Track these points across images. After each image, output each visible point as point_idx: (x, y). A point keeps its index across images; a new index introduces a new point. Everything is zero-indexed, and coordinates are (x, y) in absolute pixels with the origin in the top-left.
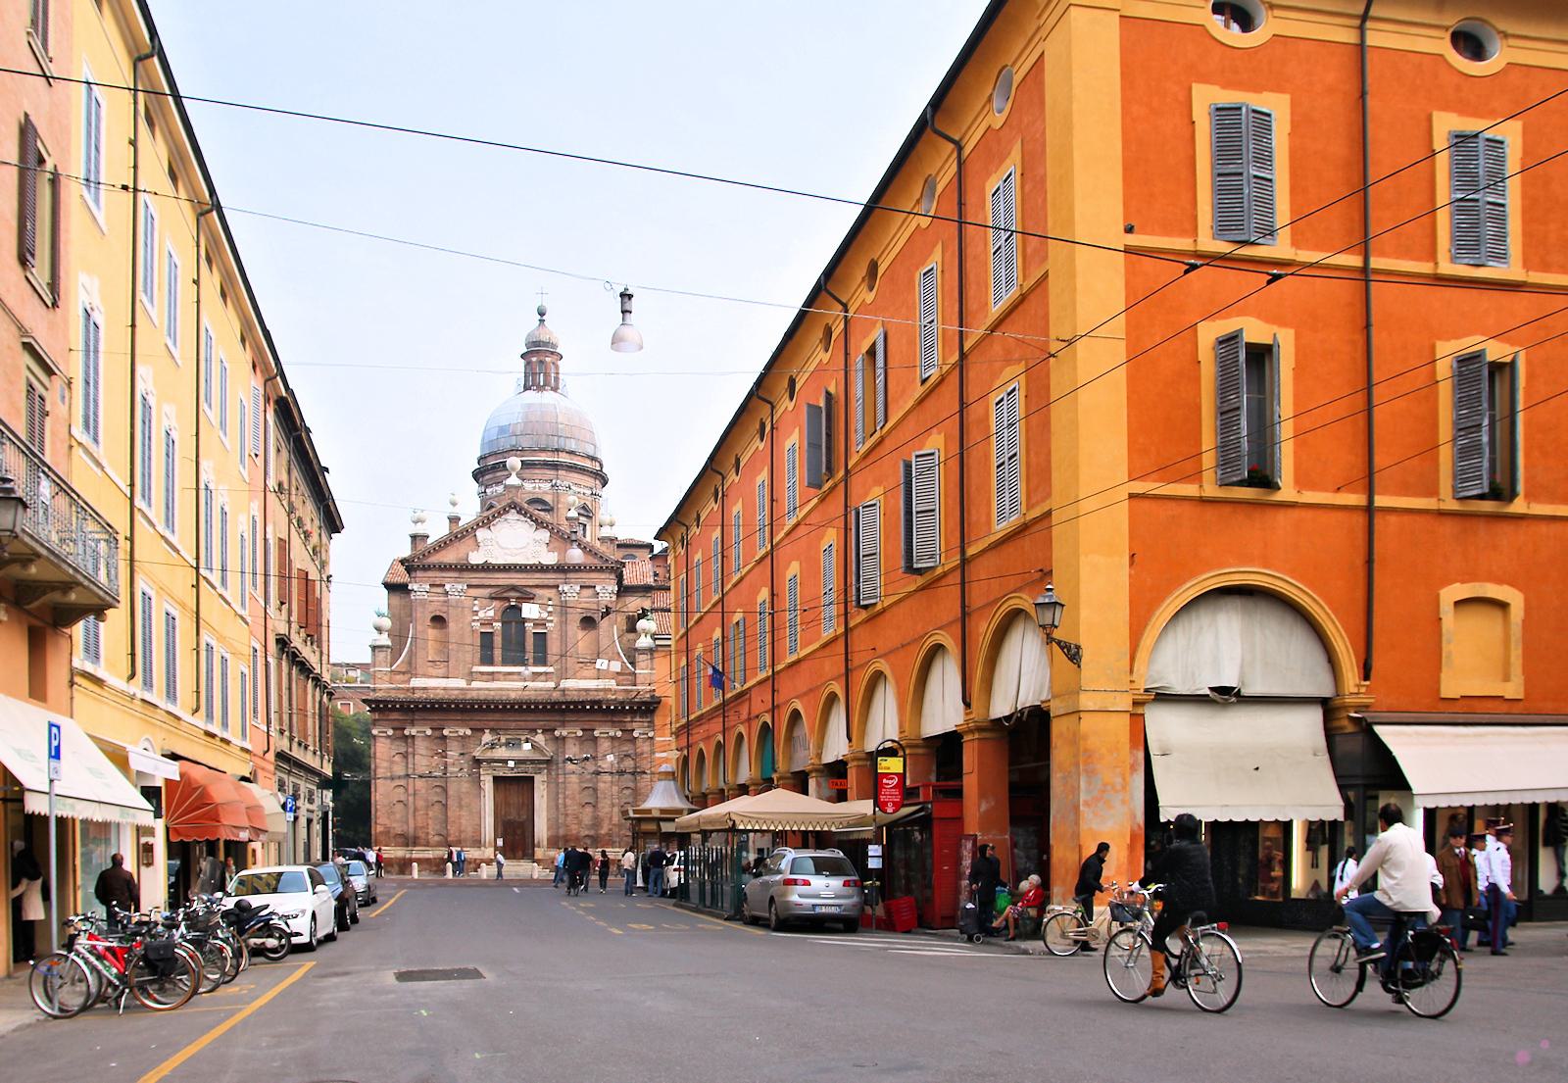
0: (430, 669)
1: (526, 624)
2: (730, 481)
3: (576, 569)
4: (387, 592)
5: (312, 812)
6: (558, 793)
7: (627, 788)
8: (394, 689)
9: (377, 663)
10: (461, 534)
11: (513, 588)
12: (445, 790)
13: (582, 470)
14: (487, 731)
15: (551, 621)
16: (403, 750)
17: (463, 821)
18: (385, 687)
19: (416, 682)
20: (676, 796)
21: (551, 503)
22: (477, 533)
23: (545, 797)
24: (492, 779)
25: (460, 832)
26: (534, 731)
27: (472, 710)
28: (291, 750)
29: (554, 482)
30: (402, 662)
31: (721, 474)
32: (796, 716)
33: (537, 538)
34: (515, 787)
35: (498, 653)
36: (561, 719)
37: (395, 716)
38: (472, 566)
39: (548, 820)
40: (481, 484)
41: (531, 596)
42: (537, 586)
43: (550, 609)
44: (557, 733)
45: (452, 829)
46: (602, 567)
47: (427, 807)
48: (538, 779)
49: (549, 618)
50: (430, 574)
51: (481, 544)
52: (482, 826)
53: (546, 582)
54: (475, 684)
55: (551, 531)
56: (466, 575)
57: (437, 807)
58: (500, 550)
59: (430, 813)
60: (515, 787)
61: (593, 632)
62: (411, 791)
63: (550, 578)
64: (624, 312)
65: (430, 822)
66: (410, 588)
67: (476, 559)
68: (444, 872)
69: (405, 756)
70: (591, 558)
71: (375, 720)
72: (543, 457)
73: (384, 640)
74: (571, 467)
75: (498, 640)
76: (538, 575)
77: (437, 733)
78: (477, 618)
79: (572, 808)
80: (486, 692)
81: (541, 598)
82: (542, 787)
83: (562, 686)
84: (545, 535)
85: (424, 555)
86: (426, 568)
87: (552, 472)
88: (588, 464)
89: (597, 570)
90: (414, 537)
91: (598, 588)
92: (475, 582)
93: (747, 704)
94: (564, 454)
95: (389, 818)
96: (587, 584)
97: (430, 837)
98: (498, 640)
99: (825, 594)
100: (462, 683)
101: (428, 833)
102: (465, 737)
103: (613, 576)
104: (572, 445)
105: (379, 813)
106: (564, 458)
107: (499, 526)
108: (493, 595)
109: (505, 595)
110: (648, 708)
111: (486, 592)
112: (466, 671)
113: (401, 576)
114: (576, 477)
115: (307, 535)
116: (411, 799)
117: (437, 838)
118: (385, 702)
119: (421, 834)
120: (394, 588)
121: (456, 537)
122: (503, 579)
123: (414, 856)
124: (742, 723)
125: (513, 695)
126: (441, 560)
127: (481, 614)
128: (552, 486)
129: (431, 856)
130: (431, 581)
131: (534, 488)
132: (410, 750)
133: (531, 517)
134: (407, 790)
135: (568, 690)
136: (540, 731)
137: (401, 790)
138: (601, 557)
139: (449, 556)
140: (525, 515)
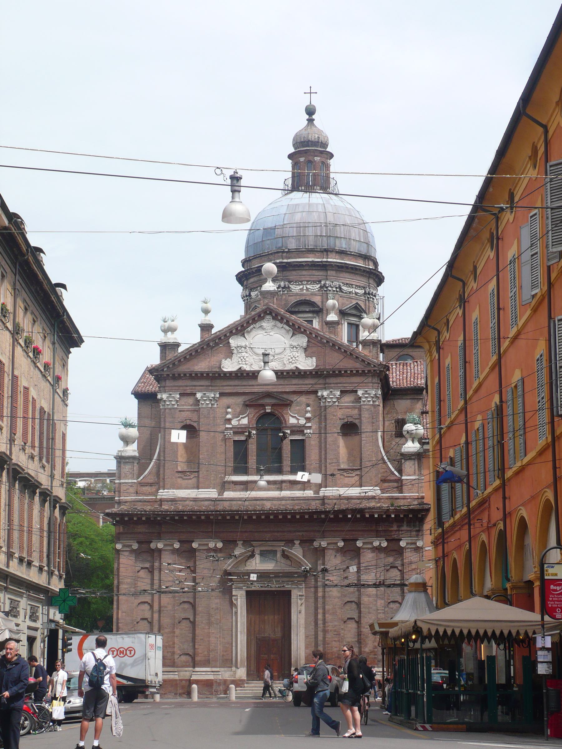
0: (179, 480)
2: (470, 288)
4: (136, 401)
5: (36, 629)
8: (140, 501)
9: (123, 475)
10: (215, 342)
12: (194, 606)
13: (354, 270)
14: (240, 543)
15: (310, 428)
16: (147, 565)
17: (212, 639)
18: (130, 499)
19: (164, 494)
20: (427, 609)
21: (319, 304)
22: (231, 341)
23: (303, 612)
25: (209, 651)
26: (290, 542)
28: (8, 566)
29: (323, 282)
30: (150, 473)
31: (461, 280)
32: (523, 525)
33: (295, 344)
34: (270, 603)
37: (141, 529)
38: (225, 373)
39: (307, 637)
40: (245, 287)
42: (294, 393)
43: (308, 415)
44: (316, 544)
45: (200, 648)
47: (173, 626)
50: (180, 383)
51: (235, 351)
52: (234, 644)
53: (304, 388)
54: (228, 494)
55: (309, 336)
56: (218, 382)
57: (185, 625)
58: (255, 357)
59: (177, 632)
60: (270, 603)
61: (357, 438)
62: (156, 607)
64: (233, 191)
65: (176, 640)
66: (159, 397)
67: (229, 366)
68: (189, 694)
69: (151, 571)
70: (351, 361)
71: (119, 533)
72: (310, 259)
73: (132, 450)
74: (342, 267)
75: (252, 447)
76: (295, 381)
77: (186, 546)
78: (231, 426)
79: (333, 623)
82: (299, 601)
83: (321, 494)
84: (303, 340)
85: (174, 364)
86: (176, 377)
87: (321, 273)
88: (360, 263)
89: (358, 374)
90: (165, 347)
91: (360, 393)
92: (228, 390)
93: (486, 514)
94: (334, 254)
96: (348, 389)
97: (176, 656)
98: (252, 447)
99: (539, 402)
100: (212, 493)
101: (173, 653)
102: (216, 550)
103: (376, 380)
104: (342, 245)
106: (333, 259)
107: (254, 333)
108: (248, 403)
109: (261, 402)
110: (414, 517)
111: (240, 400)
113: (152, 386)
114: (347, 278)
115: (37, 352)
116: (156, 616)
117: (183, 658)
118: (131, 516)
120: (144, 397)
121: (208, 345)
124: (483, 531)
125: (268, 505)
126: (192, 369)
127: (234, 422)
128: (321, 287)
129: (177, 677)
131: (302, 289)
132: (156, 564)
133: (287, 323)
134: (152, 607)
135: (328, 498)
137: (146, 607)
138: (363, 361)
139: (202, 365)
140: (281, 321)
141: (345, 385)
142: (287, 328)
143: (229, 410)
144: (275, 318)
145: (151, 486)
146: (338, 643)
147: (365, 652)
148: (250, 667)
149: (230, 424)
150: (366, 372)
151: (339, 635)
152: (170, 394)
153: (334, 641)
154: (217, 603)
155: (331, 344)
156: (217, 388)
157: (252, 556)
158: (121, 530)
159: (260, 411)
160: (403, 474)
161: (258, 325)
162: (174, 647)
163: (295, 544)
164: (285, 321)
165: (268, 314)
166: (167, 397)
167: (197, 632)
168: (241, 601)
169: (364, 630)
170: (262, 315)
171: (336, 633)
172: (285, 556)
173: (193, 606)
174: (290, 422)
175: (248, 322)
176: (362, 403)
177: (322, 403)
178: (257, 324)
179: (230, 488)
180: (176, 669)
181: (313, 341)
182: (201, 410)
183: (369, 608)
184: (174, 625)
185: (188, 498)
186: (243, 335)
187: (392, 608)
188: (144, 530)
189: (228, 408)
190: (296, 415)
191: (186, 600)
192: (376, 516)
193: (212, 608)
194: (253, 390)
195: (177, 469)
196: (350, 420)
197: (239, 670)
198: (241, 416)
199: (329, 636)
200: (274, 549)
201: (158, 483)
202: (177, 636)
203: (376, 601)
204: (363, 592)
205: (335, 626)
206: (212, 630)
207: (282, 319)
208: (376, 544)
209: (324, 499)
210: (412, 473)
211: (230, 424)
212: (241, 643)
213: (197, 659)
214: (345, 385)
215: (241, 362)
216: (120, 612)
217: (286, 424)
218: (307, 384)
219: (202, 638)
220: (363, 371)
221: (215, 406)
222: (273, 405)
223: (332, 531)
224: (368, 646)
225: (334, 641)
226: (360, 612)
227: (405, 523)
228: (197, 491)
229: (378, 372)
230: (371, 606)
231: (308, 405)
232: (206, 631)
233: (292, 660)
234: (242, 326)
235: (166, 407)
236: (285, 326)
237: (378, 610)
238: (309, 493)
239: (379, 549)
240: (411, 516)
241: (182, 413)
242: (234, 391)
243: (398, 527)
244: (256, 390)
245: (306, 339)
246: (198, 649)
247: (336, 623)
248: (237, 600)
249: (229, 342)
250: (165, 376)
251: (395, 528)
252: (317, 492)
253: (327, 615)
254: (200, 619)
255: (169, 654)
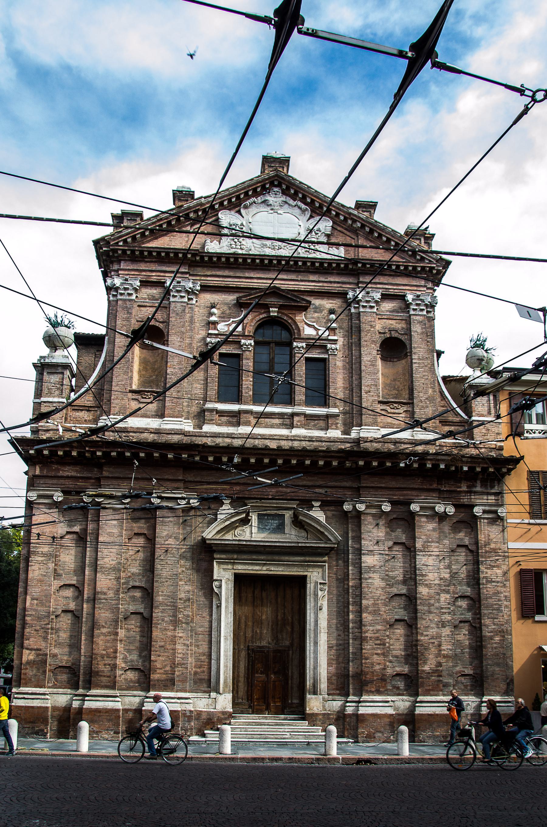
1: (295, 344)
3: (377, 269)
6: (346, 605)
7: (463, 597)
9: (45, 391)
11: (274, 292)
16: (77, 529)
24: (232, 578)
25: (174, 665)
27: (204, 467)
35: (247, 382)
36: (355, 485)
39: (330, 648)
41: (304, 304)
44: (347, 507)
45: (159, 660)
46: (415, 268)
47: (116, 621)
48: (314, 576)
49: (330, 338)
53: (327, 287)
57: (134, 624)
59: (122, 633)
61: (401, 365)
63: (333, 283)
71: (35, 476)
78: (216, 332)
79: (372, 626)
80: (228, 440)
81: (318, 309)
95: (45, 638)
96: (391, 292)
97: (119, 672)
101: (114, 667)
105: (27, 630)
107: (253, 210)
112: (194, 409)
119: (101, 666)
122: (259, 281)
123: (88, 705)
129: (118, 706)
130: (143, 276)
133: (303, 200)
136: (317, 504)
140: (294, 197)
141: (387, 287)
142: (303, 206)
143: (214, 310)
144: (284, 193)
145: (88, 411)
146: (382, 658)
147: (423, 671)
148: (237, 692)
149: (215, 328)
150: (419, 269)
151: (384, 644)
152: (126, 280)
153: (377, 654)
154: (188, 592)
155: (367, 229)
156: (198, 278)
157: (246, 521)
158: (38, 472)
159: (261, 314)
160: (474, 414)
161: (260, 199)
162: (116, 657)
163: (313, 506)
164: (300, 196)
165: (276, 186)
166: (122, 284)
167: (154, 634)
168: (227, 589)
169: (422, 638)
170: (267, 186)
171: (378, 642)
172: (297, 523)
173: (148, 594)
174: (305, 333)
175: (246, 194)
176: (412, 312)
177: (353, 310)
178: (259, 198)
179: (212, 420)
180: (118, 693)
181: (339, 228)
182: (173, 305)
183: (430, 605)
184: (118, 622)
185: (146, 429)
186: (239, 212)
187: (461, 607)
188: (74, 474)
189: (213, 306)
190: (315, 324)
191: (137, 584)
192: (442, 466)
193: (180, 599)
194: (251, 285)
195: (132, 387)
196: (394, 334)
197: (223, 696)
198: (232, 320)
199: (368, 647)
200: (280, 512)
201: (100, 407)
202: (121, 641)
203: (439, 594)
204: (420, 580)
205: (378, 631)
206: (180, 633)
207: (296, 193)
208: (440, 508)
209: (358, 441)
210: (485, 413)
211: (215, 328)
212: (226, 656)
213: (155, 676)
214: (387, 287)
215: (234, 246)
216: (28, 598)
217: (300, 335)
218: (331, 282)
219: (162, 644)
220: (415, 268)
221: (194, 302)
222: (281, 307)
223: (372, 487)
224: (429, 662)
225: (377, 654)
226: (416, 611)
227: (478, 482)
228: (161, 420)
229: (434, 272)
230: (432, 602)
231: (332, 312)
232: (169, 633)
233: (308, 683)
234: (238, 197)
235: (119, 297)
236: (299, 203)
237: (442, 608)
238: (335, 433)
239: (443, 517)
240: (491, 470)
241: (142, 308)
242: (223, 284)
243: (468, 487)
244: (255, 285)
245: (331, 223)
246: (156, 661)
247: (379, 627)
248: (220, 587)
249: (218, 219)
250: (120, 252)
251: (464, 488)
252: (346, 432)
253: (364, 615)
254: (160, 614)
255: (108, 668)
